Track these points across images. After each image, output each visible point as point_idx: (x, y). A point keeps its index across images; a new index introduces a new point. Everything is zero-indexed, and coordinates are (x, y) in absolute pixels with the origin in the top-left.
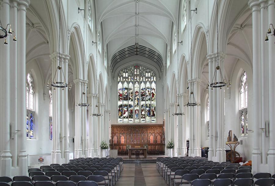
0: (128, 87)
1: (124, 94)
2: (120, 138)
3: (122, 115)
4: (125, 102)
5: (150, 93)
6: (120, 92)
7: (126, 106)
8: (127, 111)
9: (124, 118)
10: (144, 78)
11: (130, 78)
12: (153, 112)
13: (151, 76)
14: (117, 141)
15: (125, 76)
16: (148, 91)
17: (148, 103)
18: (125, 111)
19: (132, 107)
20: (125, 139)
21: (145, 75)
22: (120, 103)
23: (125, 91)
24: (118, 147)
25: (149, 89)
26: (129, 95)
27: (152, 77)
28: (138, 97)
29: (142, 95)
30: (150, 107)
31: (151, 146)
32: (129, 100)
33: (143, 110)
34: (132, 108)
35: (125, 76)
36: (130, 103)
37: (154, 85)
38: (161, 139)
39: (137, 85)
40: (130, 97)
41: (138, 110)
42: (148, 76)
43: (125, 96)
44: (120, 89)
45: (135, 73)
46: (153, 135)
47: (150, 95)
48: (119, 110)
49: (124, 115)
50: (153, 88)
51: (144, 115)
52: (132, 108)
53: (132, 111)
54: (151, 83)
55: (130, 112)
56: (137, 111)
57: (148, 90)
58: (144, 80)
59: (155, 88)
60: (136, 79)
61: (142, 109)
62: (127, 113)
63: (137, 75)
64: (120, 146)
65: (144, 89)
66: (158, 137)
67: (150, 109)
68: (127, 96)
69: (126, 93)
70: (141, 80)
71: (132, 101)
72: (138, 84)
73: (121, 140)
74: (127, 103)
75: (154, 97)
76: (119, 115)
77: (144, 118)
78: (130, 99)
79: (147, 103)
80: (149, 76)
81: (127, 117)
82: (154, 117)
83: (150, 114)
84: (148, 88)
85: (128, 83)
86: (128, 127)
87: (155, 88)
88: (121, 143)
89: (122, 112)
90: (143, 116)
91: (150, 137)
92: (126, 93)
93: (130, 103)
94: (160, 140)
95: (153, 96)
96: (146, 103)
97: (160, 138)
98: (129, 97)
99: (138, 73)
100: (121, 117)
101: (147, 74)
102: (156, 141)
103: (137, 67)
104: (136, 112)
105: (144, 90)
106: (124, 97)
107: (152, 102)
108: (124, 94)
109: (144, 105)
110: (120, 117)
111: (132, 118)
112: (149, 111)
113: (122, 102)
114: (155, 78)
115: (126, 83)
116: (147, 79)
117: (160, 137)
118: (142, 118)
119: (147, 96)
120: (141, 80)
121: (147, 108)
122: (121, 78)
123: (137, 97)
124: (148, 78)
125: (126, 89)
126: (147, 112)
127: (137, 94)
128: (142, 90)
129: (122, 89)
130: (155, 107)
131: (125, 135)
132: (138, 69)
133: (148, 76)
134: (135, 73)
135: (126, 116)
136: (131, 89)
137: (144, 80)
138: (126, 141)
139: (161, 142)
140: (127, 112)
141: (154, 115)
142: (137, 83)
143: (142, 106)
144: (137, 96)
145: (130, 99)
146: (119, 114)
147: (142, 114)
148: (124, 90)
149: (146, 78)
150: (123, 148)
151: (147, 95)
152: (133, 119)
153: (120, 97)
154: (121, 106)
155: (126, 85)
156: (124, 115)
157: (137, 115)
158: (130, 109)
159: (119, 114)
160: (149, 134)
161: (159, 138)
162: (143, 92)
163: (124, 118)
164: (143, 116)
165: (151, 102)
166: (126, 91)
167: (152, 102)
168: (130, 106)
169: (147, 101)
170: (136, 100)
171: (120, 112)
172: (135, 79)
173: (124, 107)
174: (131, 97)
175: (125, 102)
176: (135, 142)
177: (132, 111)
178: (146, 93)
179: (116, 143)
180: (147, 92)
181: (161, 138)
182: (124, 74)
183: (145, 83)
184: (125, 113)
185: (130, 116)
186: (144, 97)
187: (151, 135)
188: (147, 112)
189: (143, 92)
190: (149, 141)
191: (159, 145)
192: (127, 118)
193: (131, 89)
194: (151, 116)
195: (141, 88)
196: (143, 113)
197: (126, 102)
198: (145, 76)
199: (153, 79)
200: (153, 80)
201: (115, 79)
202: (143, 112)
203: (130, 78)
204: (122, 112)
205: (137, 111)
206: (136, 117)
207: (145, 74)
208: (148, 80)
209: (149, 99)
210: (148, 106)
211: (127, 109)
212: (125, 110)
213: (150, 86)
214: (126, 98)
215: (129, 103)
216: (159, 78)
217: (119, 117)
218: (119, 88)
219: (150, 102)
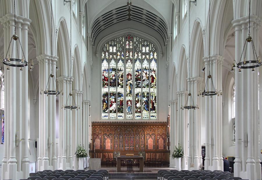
0: (117, 67)
1: (111, 77)
4: (112, 90)
5: (148, 76)
6: (105, 74)
10: (140, 55)
12: (153, 104)
13: (150, 51)
15: (113, 51)
16: (146, 74)
17: (146, 90)
21: (142, 50)
23: (111, 73)
25: (147, 70)
27: (151, 53)
28: (131, 82)
30: (148, 97)
33: (138, 101)
35: (113, 51)
37: (153, 65)
39: (129, 64)
41: (131, 101)
42: (146, 51)
50: (153, 70)
51: (140, 108)
54: (150, 61)
55: (119, 103)
56: (129, 102)
58: (140, 57)
59: (156, 68)
62: (114, 105)
63: (129, 50)
69: (114, 76)
70: (135, 58)
72: (130, 64)
75: (155, 81)
81: (116, 110)
82: (154, 111)
83: (148, 107)
84: (145, 69)
85: (117, 61)
89: (107, 104)
92: (114, 76)
95: (153, 81)
99: (131, 47)
100: (106, 111)
104: (127, 104)
105: (140, 72)
114: (155, 54)
119: (144, 80)
120: (135, 58)
122: (107, 53)
123: (129, 82)
128: (136, 71)
130: (155, 97)
133: (146, 51)
135: (113, 110)
136: (121, 70)
137: (140, 57)
144: (129, 80)
145: (120, 84)
146: (103, 106)
149: (143, 54)
151: (144, 79)
155: (113, 64)
158: (119, 99)
162: (138, 74)
165: (150, 90)
167: (151, 89)
169: (145, 87)
171: (105, 103)
172: (127, 56)
173: (111, 96)
174: (121, 81)
175: (112, 90)
177: (122, 102)
178: (143, 77)
180: (145, 74)
182: (111, 48)
183: (142, 61)
184: (111, 105)
192: (115, 112)
193: (121, 70)
195: (136, 68)
196: (138, 105)
198: (141, 51)
199: (153, 56)
200: (154, 57)
202: (137, 104)
205: (129, 102)
206: (127, 111)
208: (146, 57)
210: (146, 95)
213: (148, 66)
216: (161, 55)
217: (103, 111)
218: (103, 68)
219: (148, 89)
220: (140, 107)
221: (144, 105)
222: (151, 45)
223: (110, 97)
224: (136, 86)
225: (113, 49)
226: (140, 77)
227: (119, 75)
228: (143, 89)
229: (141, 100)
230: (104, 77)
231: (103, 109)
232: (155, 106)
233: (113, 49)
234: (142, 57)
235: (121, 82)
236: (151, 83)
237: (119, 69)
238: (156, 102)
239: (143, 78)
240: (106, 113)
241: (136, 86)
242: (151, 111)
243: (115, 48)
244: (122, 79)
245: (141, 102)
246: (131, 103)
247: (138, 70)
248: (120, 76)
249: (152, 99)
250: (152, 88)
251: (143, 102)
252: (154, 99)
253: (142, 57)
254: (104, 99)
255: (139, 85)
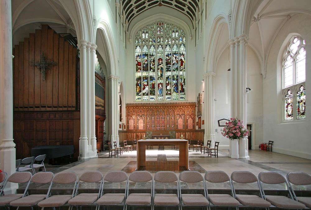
1: (144, 62)
2: (137, 122)
3: (140, 91)
4: (145, 74)
6: (138, 59)
7: (146, 78)
8: (148, 85)
9: (144, 94)
10: (170, 40)
11: (151, 40)
12: (182, 86)
14: (134, 126)
15: (145, 37)
16: (176, 58)
17: (175, 73)
18: (144, 85)
19: (154, 80)
20: (144, 123)
22: (139, 74)
23: (144, 58)
24: (135, 134)
25: (176, 54)
26: (150, 64)
28: (161, 66)
29: (167, 63)
31: (180, 133)
32: (150, 70)
33: (168, 84)
34: (153, 82)
35: (145, 37)
36: (151, 74)
38: (193, 122)
40: (151, 66)
41: (162, 84)
42: (175, 36)
43: (145, 66)
44: (138, 56)
45: (159, 33)
46: (183, 117)
47: (178, 63)
48: (137, 85)
49: (144, 91)
50: (182, 54)
51: (170, 90)
52: (153, 82)
53: (153, 85)
55: (151, 86)
56: (160, 85)
57: (175, 56)
60: (159, 42)
61: (167, 83)
62: (147, 88)
64: (137, 134)
65: (170, 54)
66: (189, 120)
67: (178, 82)
68: (147, 65)
69: (147, 61)
71: (154, 71)
72: (161, 49)
73: (139, 124)
74: (148, 74)
75: (184, 65)
76: (137, 91)
77: (170, 94)
78: (151, 68)
79: (174, 74)
80: (177, 36)
81: (148, 93)
82: (183, 93)
83: (177, 89)
84: (175, 54)
85: (149, 47)
86: (148, 107)
87: (184, 53)
88: (139, 129)
90: (169, 93)
91: (179, 120)
92: (147, 61)
93: (151, 74)
94: (192, 126)
95: (182, 65)
96: (172, 74)
97: (192, 122)
98: (150, 67)
100: (140, 94)
101: (174, 34)
102: (186, 126)
103: (160, 24)
104: (159, 86)
105: (170, 56)
106: (143, 67)
107: (181, 73)
108: (144, 62)
109: (170, 77)
110: (138, 94)
111: (155, 95)
112: (176, 85)
113: (141, 73)
115: (145, 47)
116: (173, 41)
117: (192, 120)
118: (167, 94)
119: (174, 64)
121: (174, 81)
123: (160, 66)
124: (175, 39)
125: (146, 55)
126: (174, 86)
127: (161, 61)
128: (167, 56)
129: (141, 55)
130: (184, 79)
131: (145, 118)
132: (162, 28)
133: (175, 36)
134: (159, 33)
135: (146, 93)
136: (152, 55)
137: (170, 42)
138: (145, 127)
139: (194, 126)
140: (148, 87)
141: (183, 90)
142: (160, 46)
143: (168, 78)
144: (160, 64)
145: (152, 69)
146: (137, 90)
147: (167, 89)
148: (143, 57)
150: (141, 134)
151: (174, 62)
152: (155, 96)
153: (139, 67)
154: (139, 79)
155: (145, 50)
156: (144, 91)
157: (160, 91)
158: (151, 83)
159: (137, 90)
160: (177, 117)
161: (190, 121)
162: (168, 58)
163: (144, 94)
164: (169, 93)
166: (146, 58)
168: (152, 78)
169: (174, 71)
170: (159, 71)
171: (138, 87)
172: (158, 41)
174: (153, 65)
175: (145, 74)
176: (158, 128)
178: (173, 61)
179: (133, 129)
180: (174, 58)
181: (194, 121)
182: (143, 35)
183: (171, 46)
184: (144, 88)
185: (152, 93)
186: (170, 66)
187: (179, 118)
188: (174, 86)
189: (169, 60)
190: (177, 126)
191: (190, 131)
192: (147, 95)
193: (152, 55)
194: (179, 92)
195: (166, 53)
196: (168, 88)
197: (146, 73)
199: (182, 40)
201: (130, 40)
202: (168, 86)
203: (151, 40)
204: (140, 87)
205: (160, 85)
206: (159, 94)
207: (172, 35)
209: (177, 69)
211: (148, 82)
212: (144, 83)
214: (146, 69)
215: (150, 75)
216: (190, 38)
217: (137, 94)
219: (178, 72)
220: (170, 89)
221: (174, 88)
222: (181, 31)
223: (143, 81)
224: (167, 70)
225: (145, 35)
226: (170, 61)
227: (151, 60)
228: (173, 72)
229: (171, 83)
230: (138, 62)
231: (137, 92)
232: (184, 88)
233: (145, 35)
234: (172, 42)
235: (153, 67)
236: (180, 67)
237: (151, 54)
238: (185, 85)
239: (173, 62)
240: (140, 95)
241: (167, 70)
242: (180, 93)
243: (147, 35)
244: (154, 63)
245: (171, 85)
246: (162, 86)
247: (168, 54)
248: (152, 61)
249: (181, 81)
250: (181, 71)
251: (173, 84)
252: (183, 81)
253: (172, 42)
254: (138, 83)
255: (169, 68)
